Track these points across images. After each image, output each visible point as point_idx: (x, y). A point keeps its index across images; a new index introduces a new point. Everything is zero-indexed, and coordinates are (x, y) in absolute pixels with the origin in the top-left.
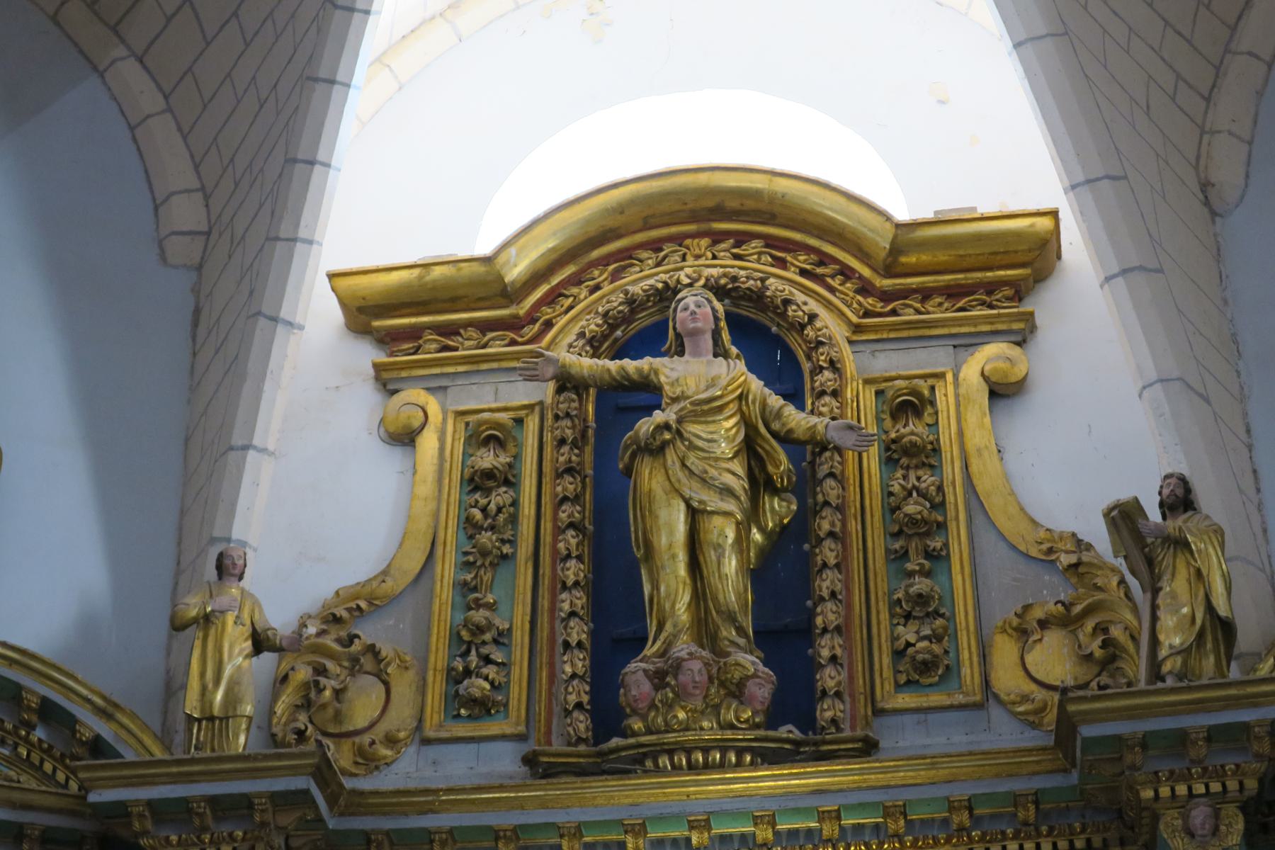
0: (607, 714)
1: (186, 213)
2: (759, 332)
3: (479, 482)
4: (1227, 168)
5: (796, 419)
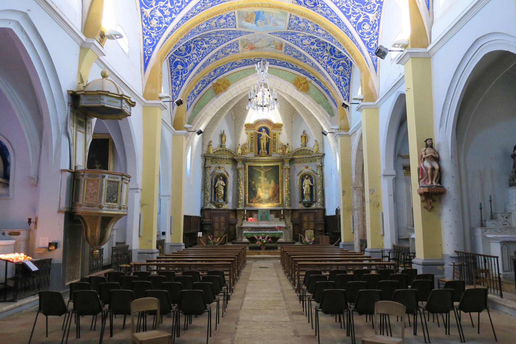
0: (259, 153)
1: (234, 117)
2: (268, 131)
3: (252, 138)
4: (293, 120)
5: (269, 137)
